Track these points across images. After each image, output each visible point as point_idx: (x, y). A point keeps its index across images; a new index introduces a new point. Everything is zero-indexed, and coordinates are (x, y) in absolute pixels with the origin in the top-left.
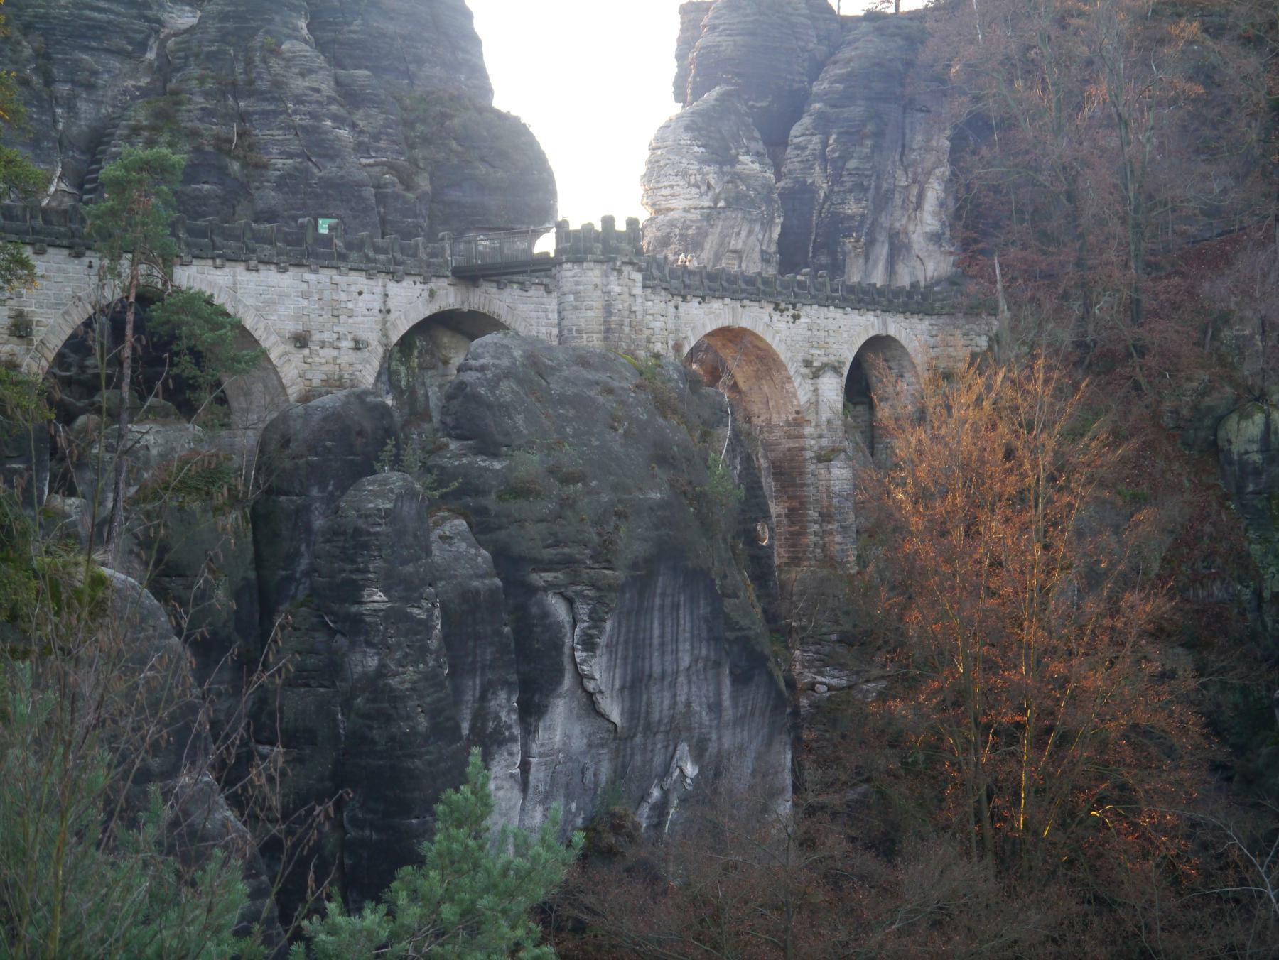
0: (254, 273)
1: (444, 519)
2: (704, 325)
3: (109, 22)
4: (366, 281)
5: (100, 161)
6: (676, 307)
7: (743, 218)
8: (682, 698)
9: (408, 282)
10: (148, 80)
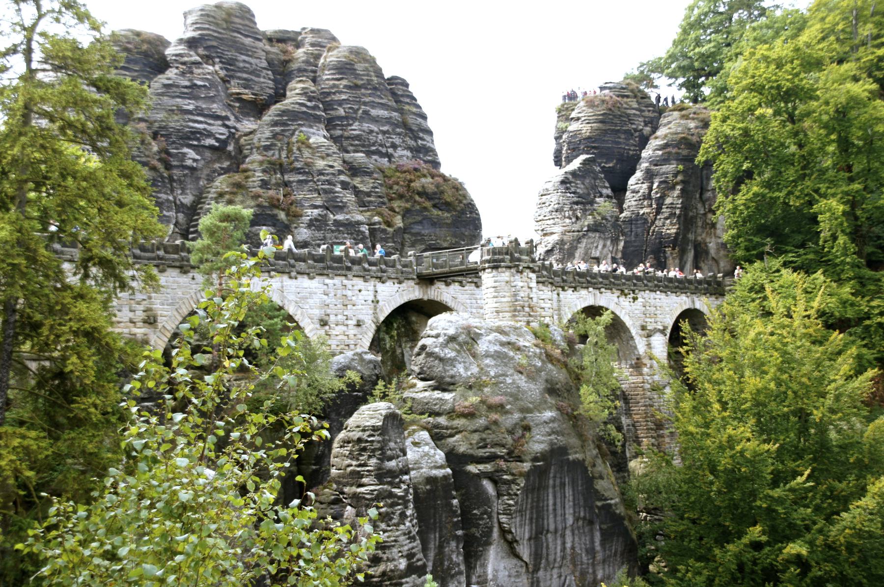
0: (294, 280)
1: (414, 431)
2: (576, 305)
3: (205, 129)
4: (364, 283)
5: (199, 214)
6: (558, 294)
7: (599, 237)
8: (569, 545)
9: (389, 283)
10: (228, 163)
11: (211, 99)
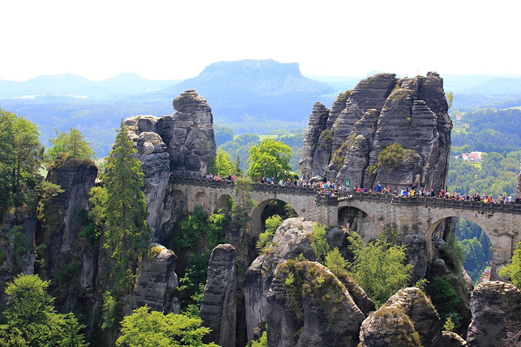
2: (442, 215)
6: (429, 210)
11: (352, 118)
